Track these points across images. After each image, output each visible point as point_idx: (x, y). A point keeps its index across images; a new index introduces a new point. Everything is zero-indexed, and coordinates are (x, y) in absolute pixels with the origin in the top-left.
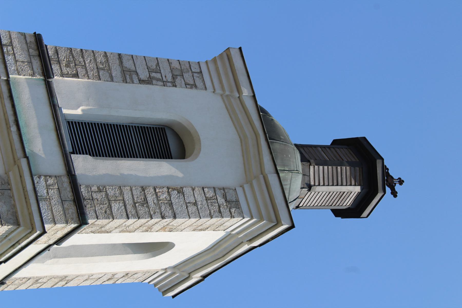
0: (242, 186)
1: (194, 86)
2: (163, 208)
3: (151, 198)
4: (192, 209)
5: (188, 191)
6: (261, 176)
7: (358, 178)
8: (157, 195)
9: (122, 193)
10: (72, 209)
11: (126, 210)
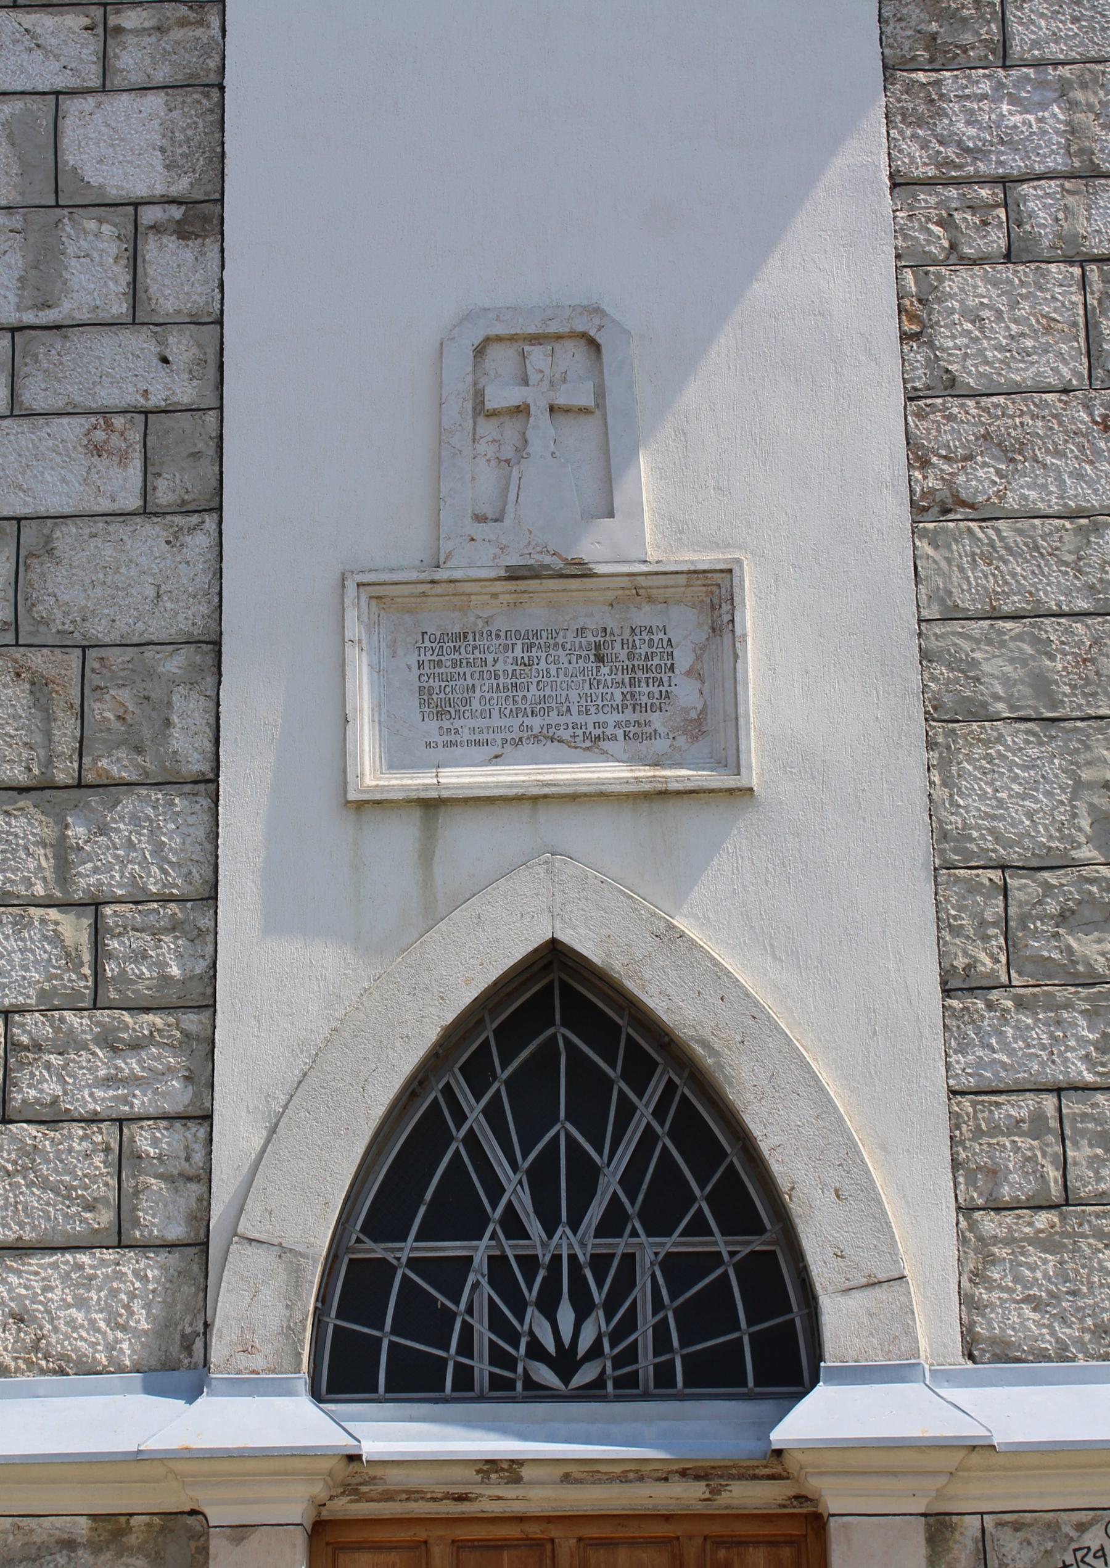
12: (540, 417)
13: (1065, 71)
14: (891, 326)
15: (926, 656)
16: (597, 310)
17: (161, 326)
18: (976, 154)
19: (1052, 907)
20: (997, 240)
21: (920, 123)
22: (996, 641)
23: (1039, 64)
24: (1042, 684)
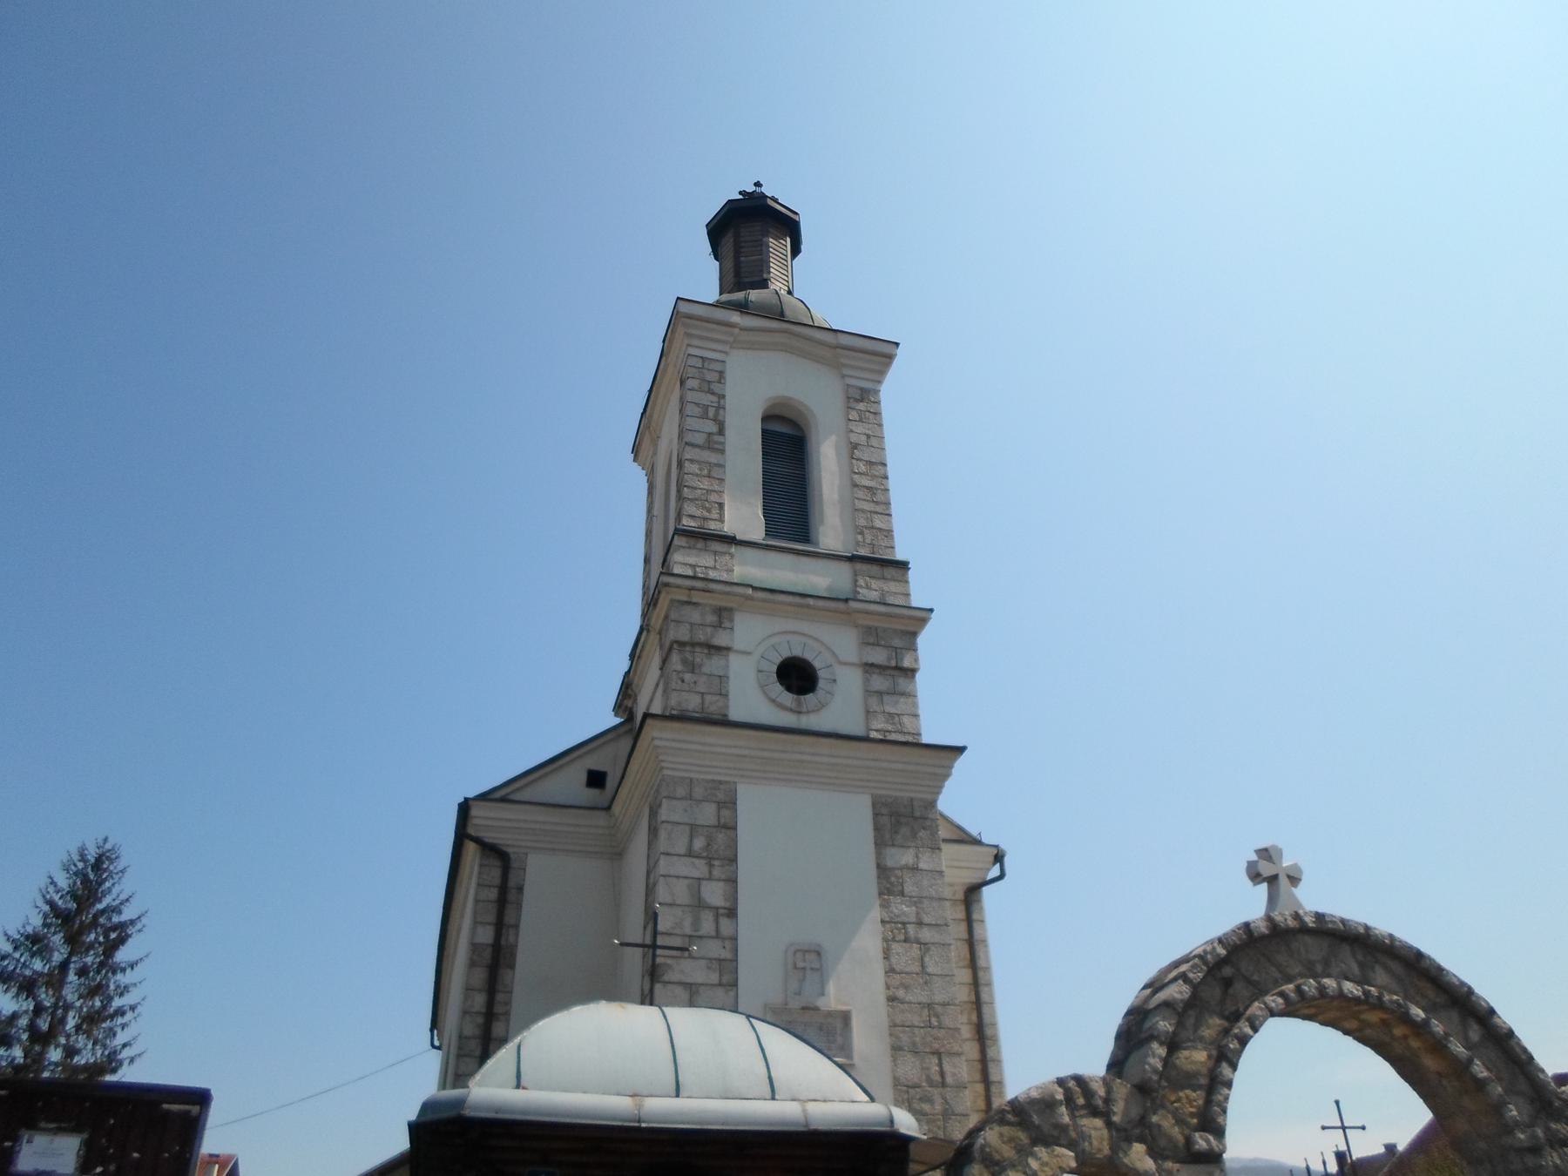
0: (843, 376)
1: (721, 373)
2: (877, 473)
3: (866, 482)
4: (874, 442)
5: (854, 438)
6: (839, 351)
7: (779, 235)
8: (861, 474)
9: (863, 511)
10: (890, 572)
11: (882, 514)
12: (808, 972)
13: (915, 899)
14: (881, 955)
15: (891, 1035)
16: (819, 945)
17: (724, 939)
18: (898, 916)
19: (918, 1097)
20: (902, 937)
21: (886, 907)
22: (904, 1032)
23: (910, 897)
24: (914, 1044)
